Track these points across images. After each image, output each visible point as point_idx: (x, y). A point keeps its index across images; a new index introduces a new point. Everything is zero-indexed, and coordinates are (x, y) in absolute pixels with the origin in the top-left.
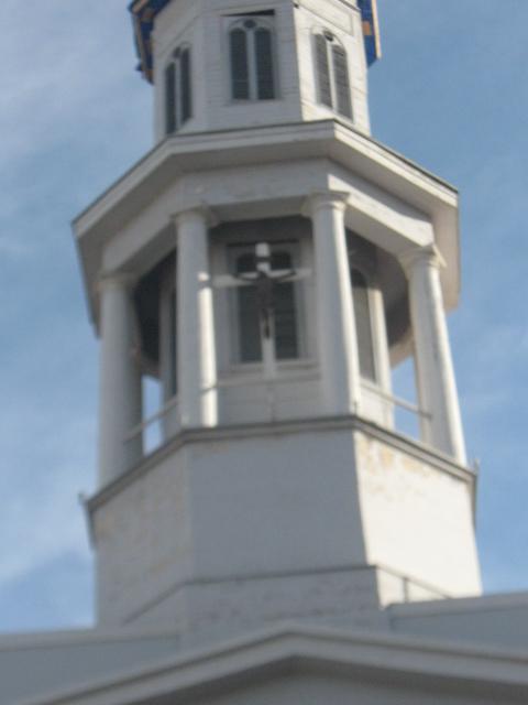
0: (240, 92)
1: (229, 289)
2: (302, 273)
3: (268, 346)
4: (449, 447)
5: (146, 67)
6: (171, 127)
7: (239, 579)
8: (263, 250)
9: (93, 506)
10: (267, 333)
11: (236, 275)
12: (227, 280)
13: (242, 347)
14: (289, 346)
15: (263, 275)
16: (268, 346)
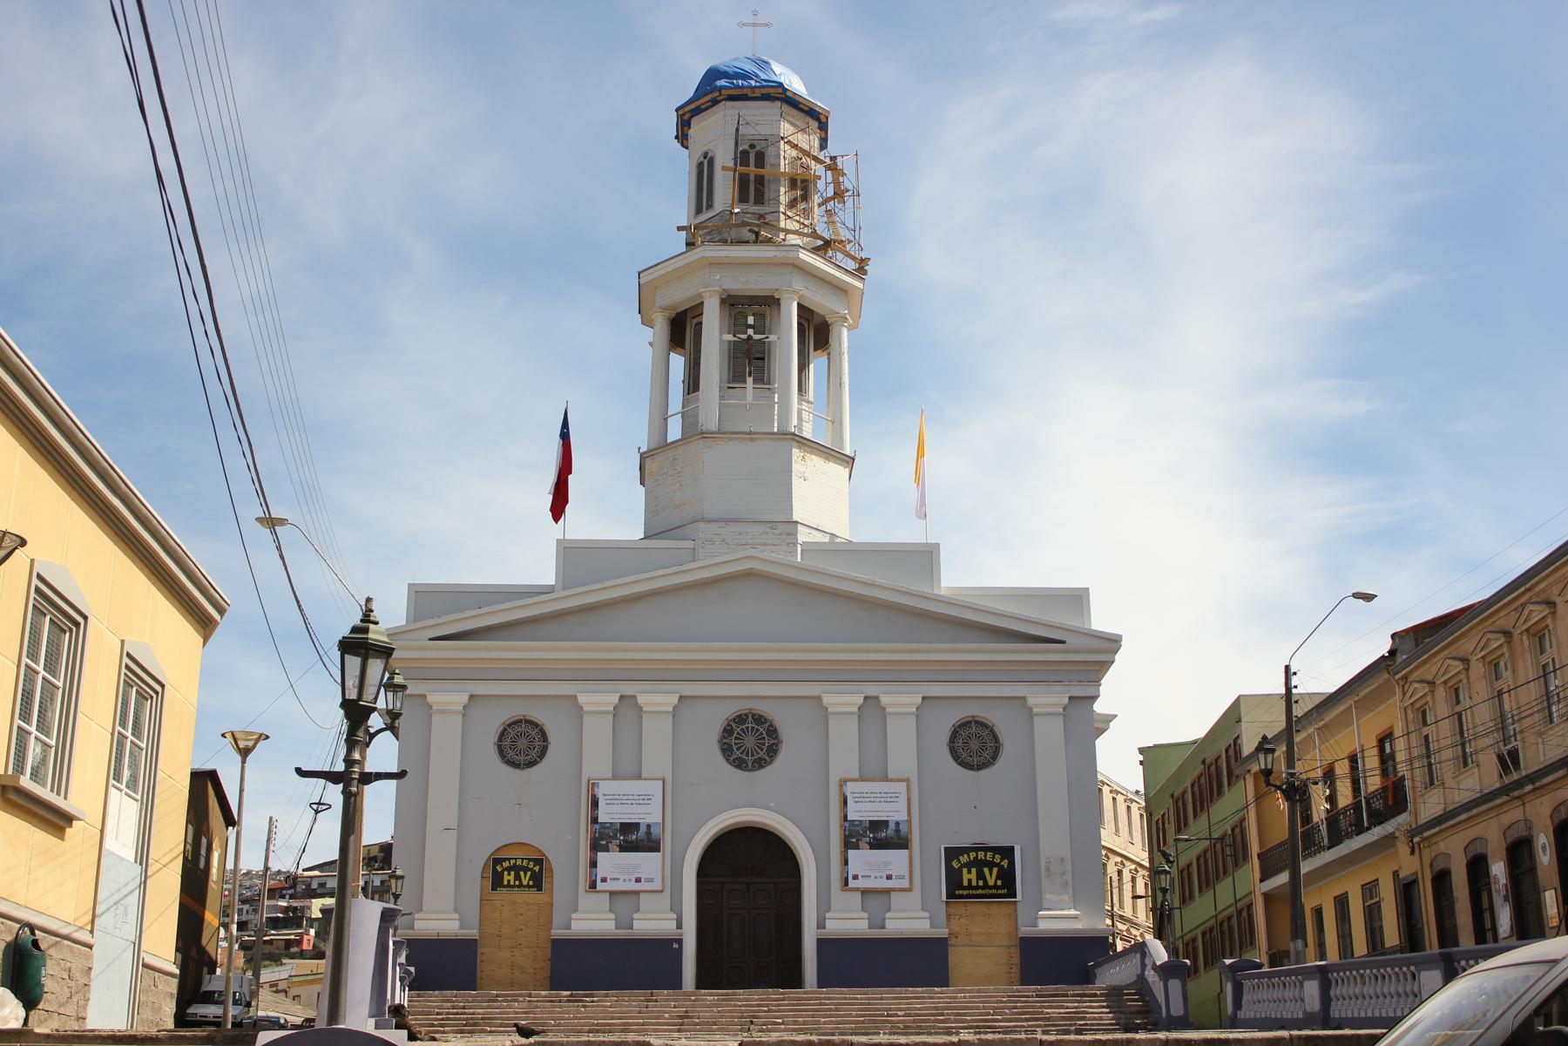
0: (743, 198)
1: (729, 342)
2: (772, 338)
3: (750, 380)
4: (842, 446)
5: (682, 138)
6: (699, 211)
7: (727, 521)
8: (751, 320)
9: (643, 458)
10: (750, 376)
11: (734, 336)
12: (730, 337)
13: (735, 376)
14: (763, 378)
15: (750, 337)
16: (750, 380)
